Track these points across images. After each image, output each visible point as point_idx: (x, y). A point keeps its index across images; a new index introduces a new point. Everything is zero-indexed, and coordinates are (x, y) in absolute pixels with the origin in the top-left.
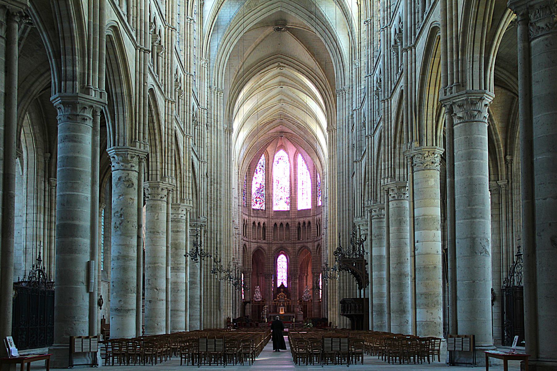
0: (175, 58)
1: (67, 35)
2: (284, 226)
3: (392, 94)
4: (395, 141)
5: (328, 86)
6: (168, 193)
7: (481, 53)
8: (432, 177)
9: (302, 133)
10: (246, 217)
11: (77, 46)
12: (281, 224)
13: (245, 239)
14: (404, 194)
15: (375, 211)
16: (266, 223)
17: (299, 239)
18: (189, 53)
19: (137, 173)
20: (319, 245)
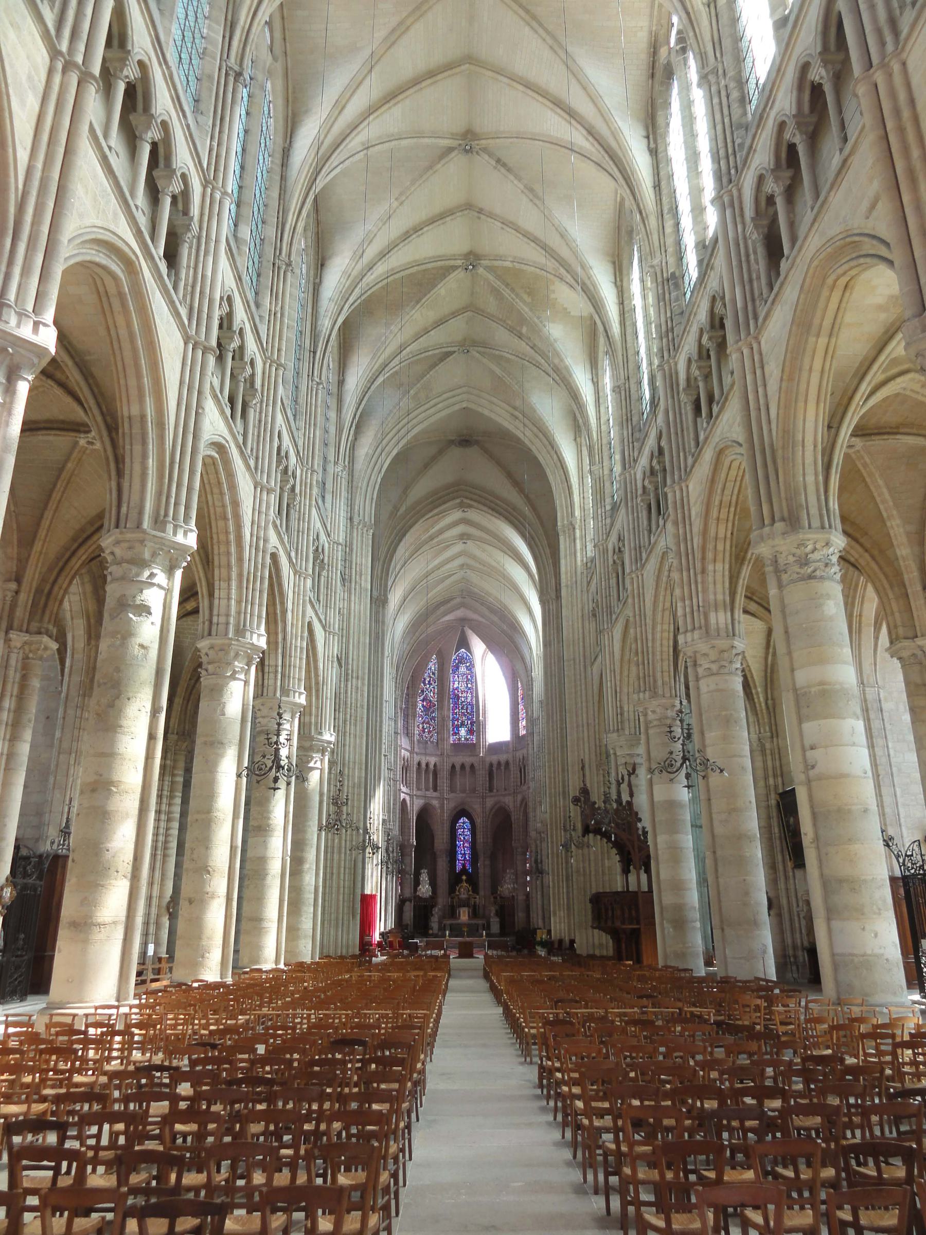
2: (468, 768)
4: (703, 558)
8: (828, 596)
9: (496, 619)
10: (407, 754)
12: (463, 766)
15: (653, 712)
17: (491, 790)
20: (523, 799)
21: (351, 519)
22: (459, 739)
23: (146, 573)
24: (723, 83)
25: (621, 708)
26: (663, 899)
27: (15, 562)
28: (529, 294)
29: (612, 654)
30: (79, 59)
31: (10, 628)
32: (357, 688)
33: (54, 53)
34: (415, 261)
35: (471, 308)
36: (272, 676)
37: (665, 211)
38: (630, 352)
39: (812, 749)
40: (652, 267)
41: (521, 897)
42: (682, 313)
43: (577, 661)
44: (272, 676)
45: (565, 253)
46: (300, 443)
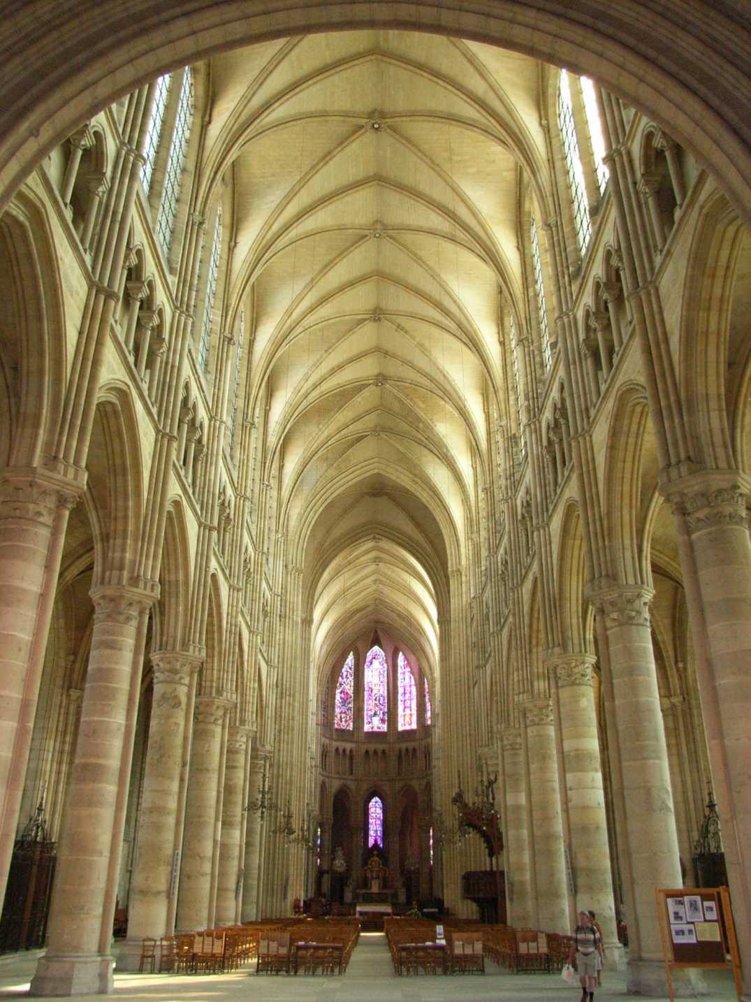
1: (120, 514)
3: (522, 581)
4: (530, 643)
5: (438, 565)
6: (225, 714)
7: (632, 539)
8: (583, 695)
10: (327, 741)
11: (131, 528)
12: (375, 752)
13: (324, 773)
14: (547, 716)
16: (354, 750)
19: (187, 688)
21: (286, 566)
22: (372, 728)
23: (179, 676)
25: (491, 727)
26: (512, 876)
27: (73, 641)
28: (424, 402)
29: (485, 684)
30: (168, 430)
31: (69, 687)
32: (289, 704)
33: (158, 431)
34: (338, 384)
37: (510, 388)
38: (494, 463)
39: (571, 789)
40: (501, 426)
41: (426, 870)
43: (463, 681)
46: (254, 533)
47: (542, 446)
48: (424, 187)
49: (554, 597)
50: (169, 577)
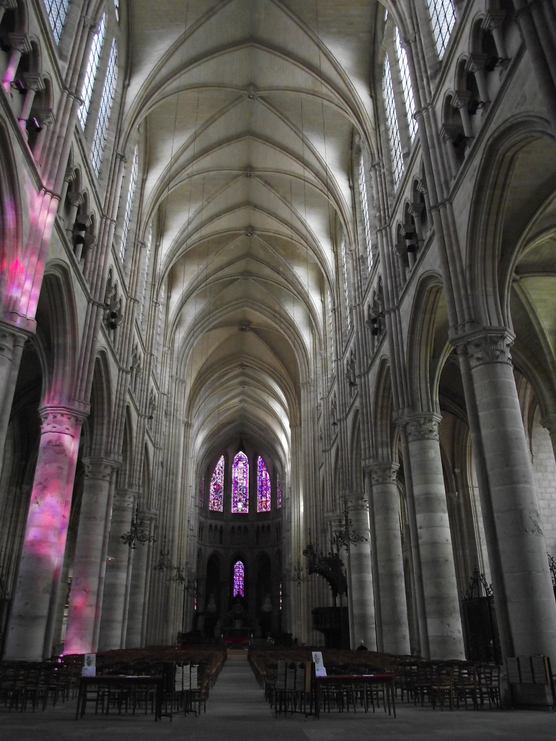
0: (134, 329)
5: (291, 384)
6: (112, 472)
7: (494, 287)
12: (239, 528)
18: (151, 334)
22: (237, 510)
24: (382, 171)
32: (173, 481)
35: (249, 255)
36: (123, 476)
42: (366, 278)
44: (123, 476)
45: (304, 231)
47: (392, 246)
48: (292, 47)
49: (404, 365)
50: (58, 341)
